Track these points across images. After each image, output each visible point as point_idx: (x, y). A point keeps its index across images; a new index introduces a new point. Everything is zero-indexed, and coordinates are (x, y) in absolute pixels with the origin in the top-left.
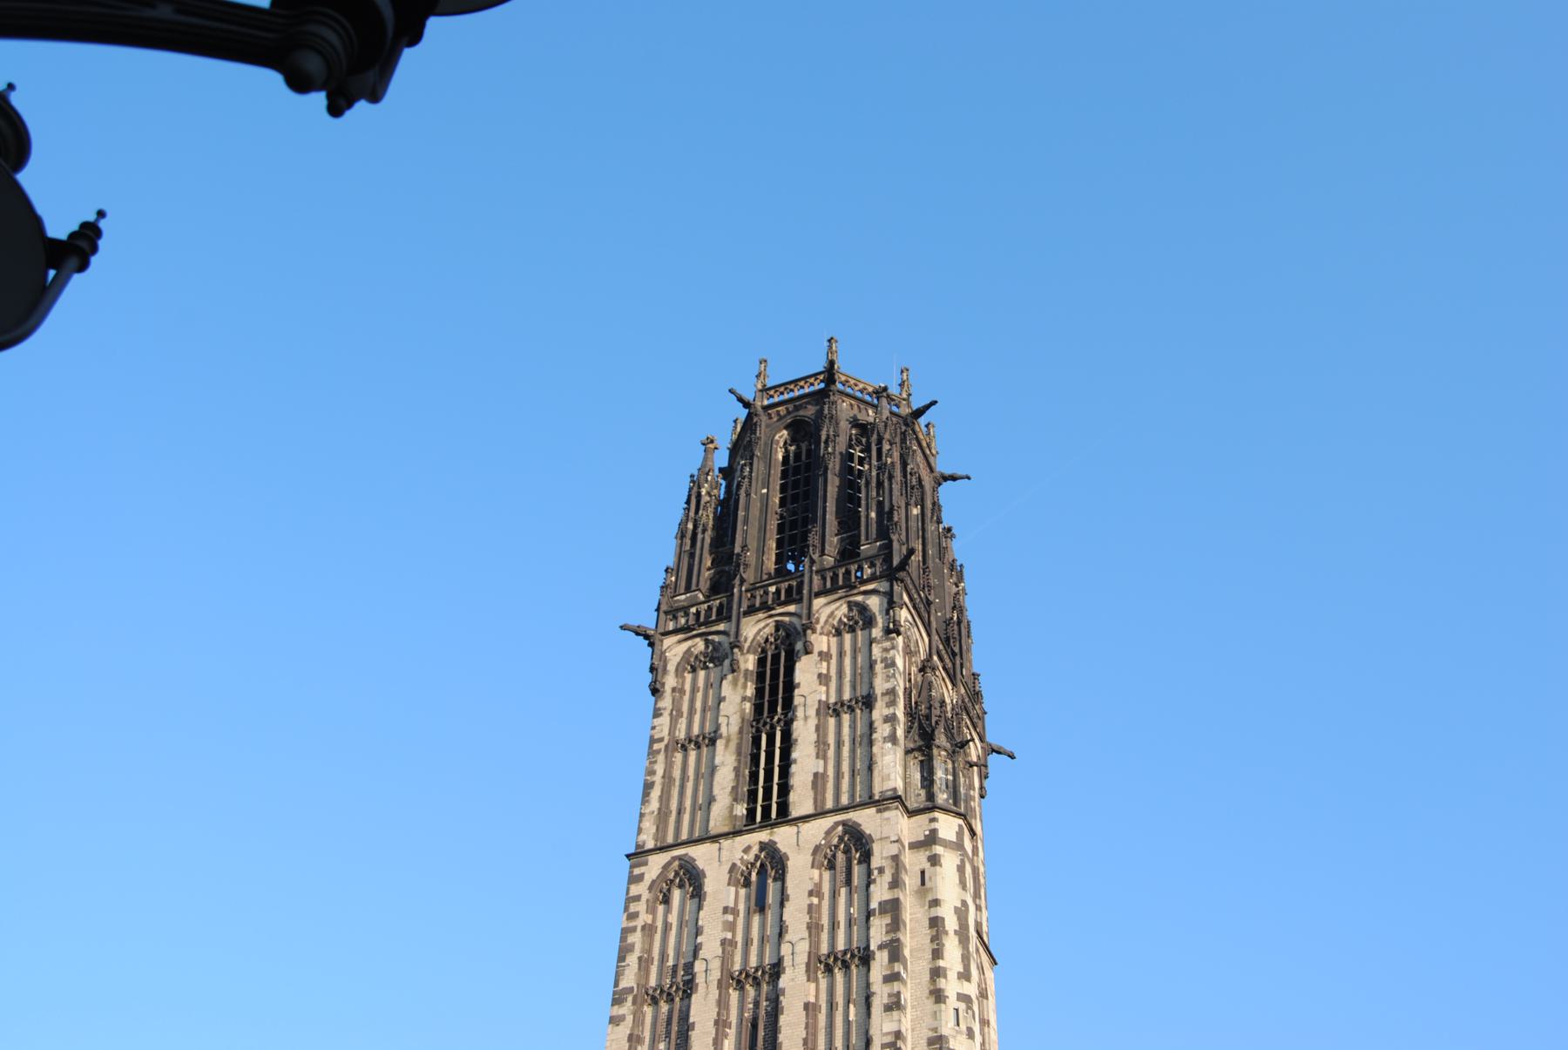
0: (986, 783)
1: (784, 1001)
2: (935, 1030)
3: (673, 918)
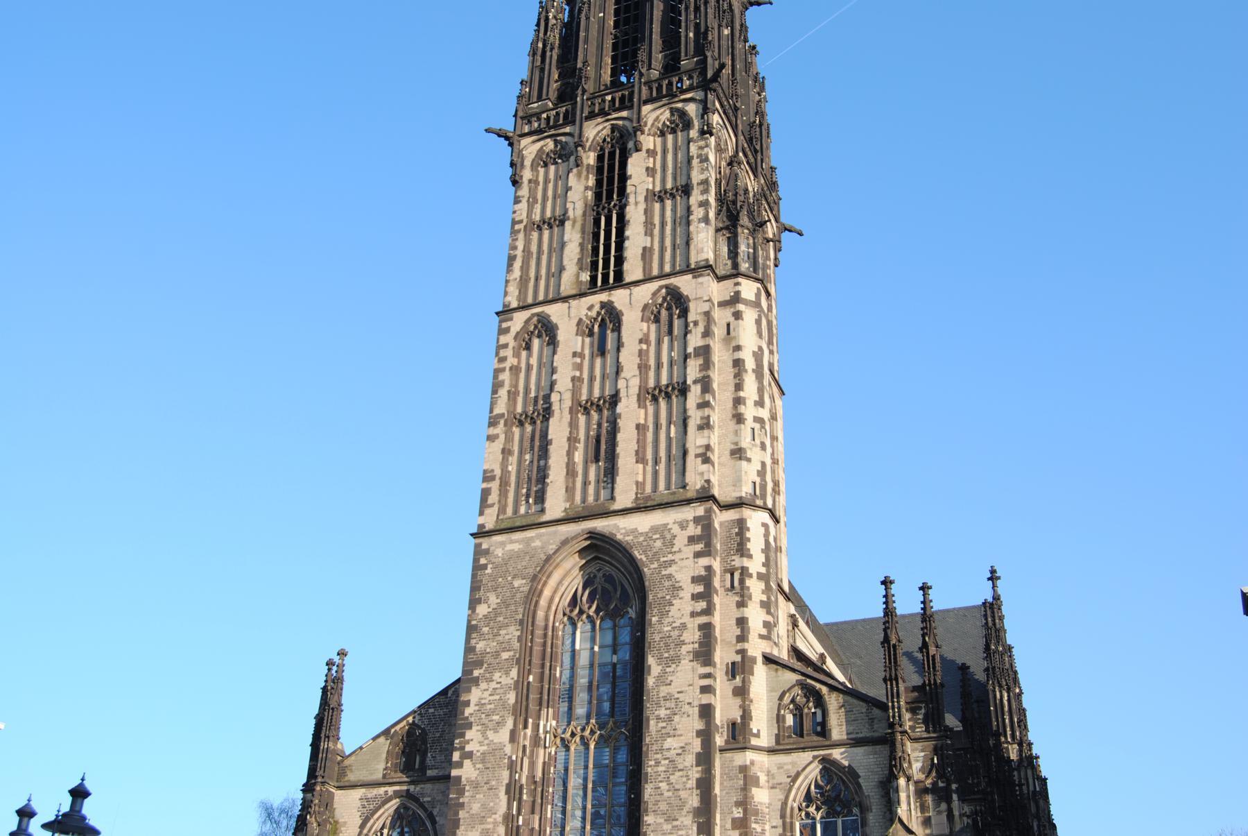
0: (780, 255)
1: (621, 423)
2: (736, 444)
3: (534, 361)
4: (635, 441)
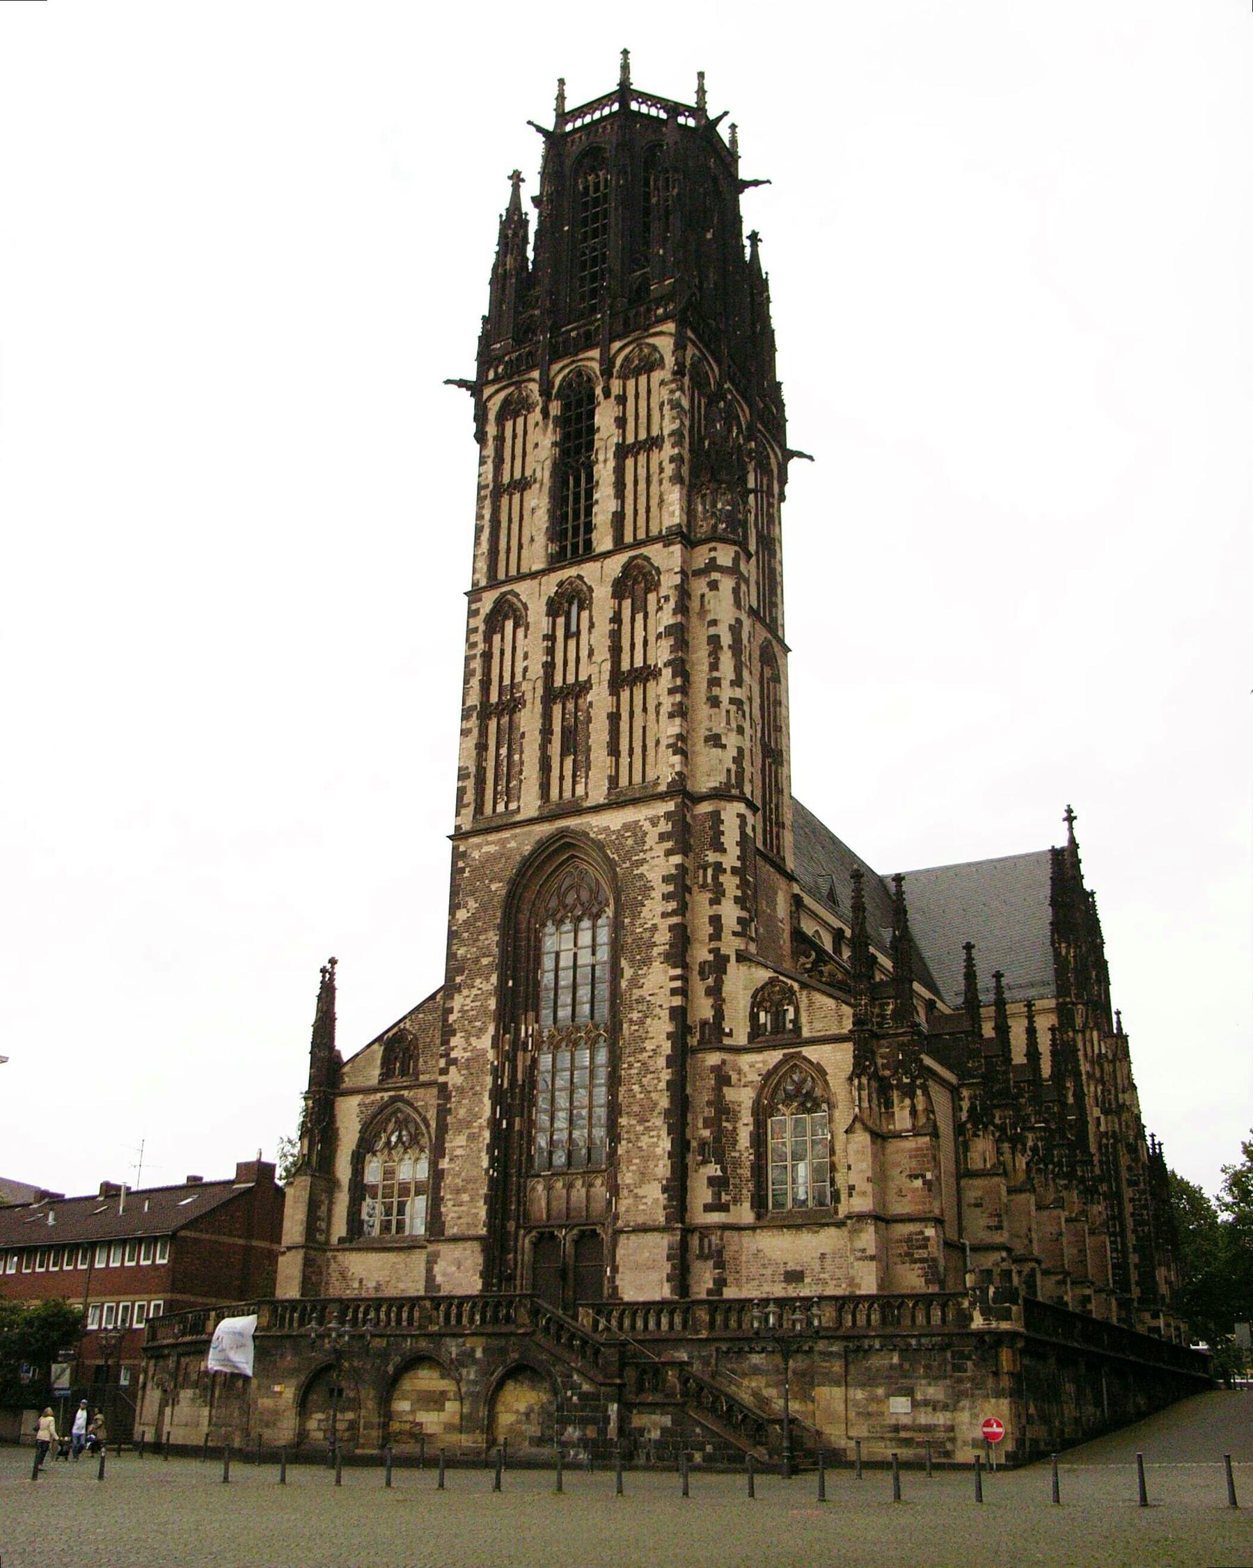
4: (607, 732)
